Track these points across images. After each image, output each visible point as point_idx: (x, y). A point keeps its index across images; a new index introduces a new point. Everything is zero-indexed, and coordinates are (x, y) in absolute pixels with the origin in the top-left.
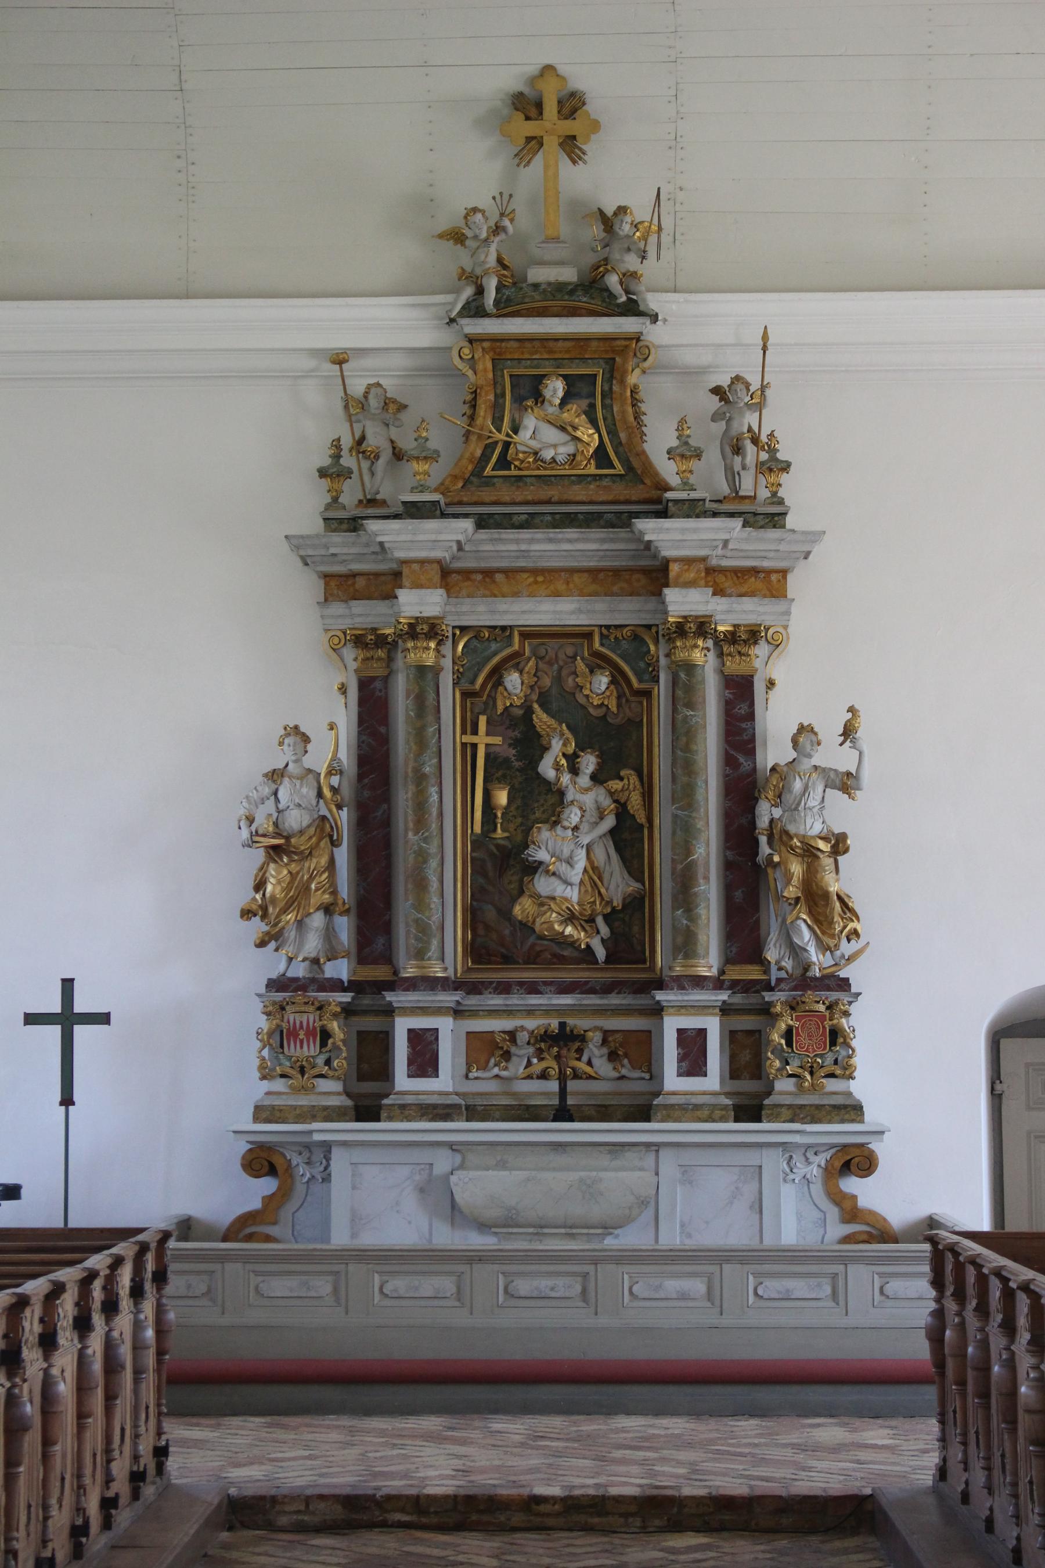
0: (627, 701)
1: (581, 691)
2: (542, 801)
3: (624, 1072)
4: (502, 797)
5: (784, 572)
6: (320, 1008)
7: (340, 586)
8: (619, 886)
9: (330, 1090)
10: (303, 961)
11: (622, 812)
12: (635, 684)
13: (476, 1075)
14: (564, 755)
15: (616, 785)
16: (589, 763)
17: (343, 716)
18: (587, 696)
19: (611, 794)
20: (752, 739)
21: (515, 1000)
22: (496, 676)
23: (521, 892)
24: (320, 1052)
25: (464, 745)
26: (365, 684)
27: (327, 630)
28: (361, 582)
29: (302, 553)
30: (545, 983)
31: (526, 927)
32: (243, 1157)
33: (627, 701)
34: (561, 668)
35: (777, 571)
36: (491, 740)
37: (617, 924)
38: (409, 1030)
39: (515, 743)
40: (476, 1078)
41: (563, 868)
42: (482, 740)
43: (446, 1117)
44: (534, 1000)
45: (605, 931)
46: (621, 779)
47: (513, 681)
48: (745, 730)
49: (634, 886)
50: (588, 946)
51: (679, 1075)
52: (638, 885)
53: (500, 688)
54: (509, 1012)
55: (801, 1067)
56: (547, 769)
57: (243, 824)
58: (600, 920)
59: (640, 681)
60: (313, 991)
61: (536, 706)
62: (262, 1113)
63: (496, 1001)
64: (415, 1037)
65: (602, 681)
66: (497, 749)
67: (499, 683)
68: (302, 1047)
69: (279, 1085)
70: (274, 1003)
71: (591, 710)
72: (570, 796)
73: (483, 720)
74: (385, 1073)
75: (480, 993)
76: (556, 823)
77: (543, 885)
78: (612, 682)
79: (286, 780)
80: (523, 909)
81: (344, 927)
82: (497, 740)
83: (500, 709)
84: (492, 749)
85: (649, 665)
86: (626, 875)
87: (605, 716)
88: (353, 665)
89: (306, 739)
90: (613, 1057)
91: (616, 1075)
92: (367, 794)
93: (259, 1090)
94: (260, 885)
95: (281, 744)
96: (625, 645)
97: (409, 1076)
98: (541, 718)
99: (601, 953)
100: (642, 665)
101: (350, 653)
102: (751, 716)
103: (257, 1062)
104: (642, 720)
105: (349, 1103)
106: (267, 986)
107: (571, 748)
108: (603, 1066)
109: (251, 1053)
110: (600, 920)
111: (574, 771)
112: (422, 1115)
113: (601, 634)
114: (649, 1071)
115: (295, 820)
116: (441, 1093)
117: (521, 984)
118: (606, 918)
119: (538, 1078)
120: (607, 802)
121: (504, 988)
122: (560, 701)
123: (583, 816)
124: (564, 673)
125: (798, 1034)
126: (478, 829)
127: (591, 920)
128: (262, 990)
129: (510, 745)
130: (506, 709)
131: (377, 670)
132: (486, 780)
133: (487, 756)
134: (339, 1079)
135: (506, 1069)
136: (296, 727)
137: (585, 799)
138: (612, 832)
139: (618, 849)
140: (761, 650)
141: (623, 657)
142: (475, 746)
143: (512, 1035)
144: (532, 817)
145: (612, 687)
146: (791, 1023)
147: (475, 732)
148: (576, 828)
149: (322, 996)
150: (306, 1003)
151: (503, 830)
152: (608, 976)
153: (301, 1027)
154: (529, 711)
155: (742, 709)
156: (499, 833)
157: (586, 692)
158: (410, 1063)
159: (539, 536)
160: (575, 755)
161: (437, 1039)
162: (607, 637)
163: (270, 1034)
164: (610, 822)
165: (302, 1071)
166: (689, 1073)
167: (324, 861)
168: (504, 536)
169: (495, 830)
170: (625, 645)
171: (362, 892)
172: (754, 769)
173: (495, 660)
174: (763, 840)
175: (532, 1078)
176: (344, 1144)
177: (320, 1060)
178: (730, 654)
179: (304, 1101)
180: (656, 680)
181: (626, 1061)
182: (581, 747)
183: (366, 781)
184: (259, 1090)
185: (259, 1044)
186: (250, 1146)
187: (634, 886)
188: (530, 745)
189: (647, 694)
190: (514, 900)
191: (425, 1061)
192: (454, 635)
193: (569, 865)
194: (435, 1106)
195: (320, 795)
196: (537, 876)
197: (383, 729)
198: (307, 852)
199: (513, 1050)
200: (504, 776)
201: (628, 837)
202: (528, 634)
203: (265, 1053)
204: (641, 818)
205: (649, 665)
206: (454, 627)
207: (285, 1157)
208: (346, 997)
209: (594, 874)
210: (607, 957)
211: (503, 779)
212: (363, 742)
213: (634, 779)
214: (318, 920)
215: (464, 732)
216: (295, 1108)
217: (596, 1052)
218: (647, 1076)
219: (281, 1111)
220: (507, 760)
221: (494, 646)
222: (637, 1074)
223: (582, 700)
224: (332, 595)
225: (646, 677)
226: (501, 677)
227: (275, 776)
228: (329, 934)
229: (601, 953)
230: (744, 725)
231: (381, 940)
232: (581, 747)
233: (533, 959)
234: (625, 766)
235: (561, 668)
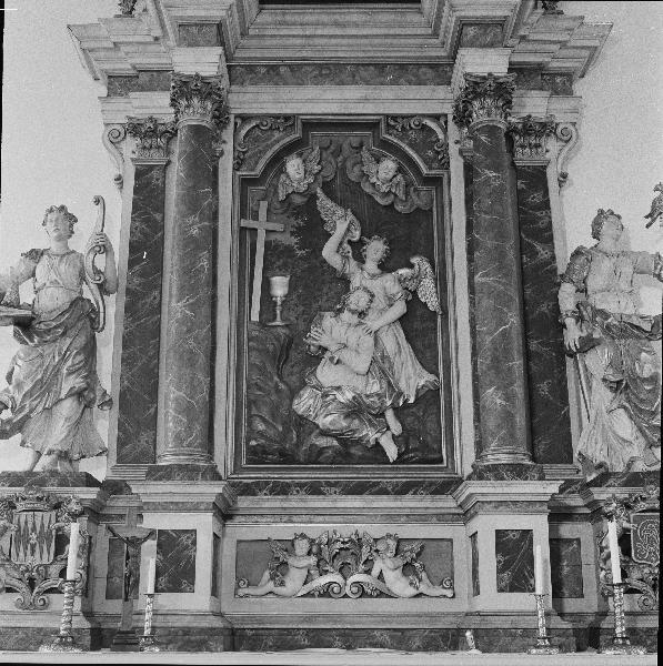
0: (415, 190)
1: (367, 180)
2: (325, 290)
3: (423, 588)
4: (280, 286)
5: (569, 76)
6: (57, 507)
7: (120, 84)
8: (412, 378)
9: (63, 611)
10: (50, 453)
11: (413, 302)
12: (425, 170)
13: (246, 591)
14: (350, 242)
15: (404, 272)
16: (376, 249)
17: (120, 207)
18: (374, 184)
19: (400, 281)
20: (549, 226)
21: (294, 502)
22: (277, 162)
23: (304, 385)
24: (55, 559)
25: (243, 230)
26: (141, 174)
27: (107, 125)
28: (144, 78)
29: (85, 45)
30: (329, 484)
31: (303, 424)
33: (415, 190)
34: (345, 160)
35: (561, 75)
36: (271, 226)
37: (409, 419)
39: (297, 232)
40: (247, 596)
41: (345, 355)
42: (261, 225)
43: (199, 646)
44: (316, 502)
45: (396, 428)
46: (411, 266)
47: (294, 166)
48: (540, 218)
49: (426, 378)
50: (377, 443)
51: (501, 590)
52: (432, 377)
53: (283, 177)
54: (289, 516)
55: (642, 580)
56: (329, 252)
58: (390, 415)
59: (430, 168)
60: (53, 485)
61: (319, 190)
63: (275, 502)
65: (388, 166)
66: (279, 237)
67: (282, 170)
71: (378, 199)
72: (356, 282)
73: (264, 205)
74: (132, 584)
75: (255, 494)
76: (340, 311)
77: (326, 374)
78: (400, 170)
79: (45, 256)
80: (305, 403)
81: (105, 427)
82: (278, 227)
83: (282, 197)
84: (273, 237)
85: (438, 153)
86: (419, 366)
87: (392, 205)
88: (128, 155)
89: (72, 219)
90: (407, 569)
91: (413, 591)
92: (136, 281)
96: (412, 135)
98: (324, 203)
99: (392, 451)
100: (430, 153)
101: (130, 145)
102: (546, 205)
104: (431, 210)
107: (356, 235)
108: (397, 582)
110: (390, 415)
111: (361, 259)
113: (388, 125)
114: (452, 587)
117: (301, 486)
118: (398, 411)
119: (320, 596)
120: (395, 289)
121: (282, 489)
122: (348, 192)
123: (371, 301)
124: (349, 164)
125: (636, 540)
126: (255, 317)
127: (382, 415)
129: (292, 234)
130: (288, 196)
131: (156, 158)
132: (265, 270)
133: (267, 245)
135: (282, 584)
136: (63, 208)
137: (375, 288)
138: (402, 320)
139: (408, 339)
140: (552, 145)
141: (410, 145)
143: (289, 546)
144: (315, 306)
145: (399, 177)
146: (625, 525)
147: (256, 218)
148: (362, 314)
150: (39, 499)
151: (283, 320)
152: (402, 477)
153: (34, 529)
154: (314, 197)
155: (537, 198)
157: (374, 180)
159: (325, 18)
160: (361, 243)
161: (194, 543)
162: (394, 127)
164: (400, 308)
165: (32, 583)
166: (513, 589)
167: (81, 341)
168: (288, 18)
169: (274, 319)
170: (412, 135)
171: (126, 382)
172: (553, 258)
173: (277, 147)
174: (570, 322)
175: (313, 596)
177: (54, 570)
178: (523, 147)
179: (32, 621)
180: (446, 166)
181: (424, 575)
182: (367, 233)
183: (137, 268)
187: (426, 378)
188: (314, 232)
189: (436, 182)
190: (294, 393)
191: (176, 574)
192: (236, 124)
193: (355, 357)
194: (187, 631)
195: (82, 278)
196: (319, 367)
197: (158, 217)
198: (61, 331)
199: (291, 561)
200: (285, 265)
201: (421, 326)
202: (312, 124)
204: (434, 304)
205: (438, 153)
206: (237, 116)
208: (91, 494)
209: (381, 366)
210: (399, 455)
211: (282, 271)
213: (426, 266)
214: (68, 407)
215: (243, 215)
217: (389, 563)
218: (449, 593)
220: (289, 250)
221: (277, 135)
222: (439, 591)
223: (368, 190)
224: (115, 93)
225: (435, 165)
226: (284, 164)
227: (35, 255)
228: (79, 425)
229: (392, 451)
230: (538, 213)
231: (144, 437)
232: (367, 233)
233: (315, 457)
234: (414, 255)
235: (345, 160)
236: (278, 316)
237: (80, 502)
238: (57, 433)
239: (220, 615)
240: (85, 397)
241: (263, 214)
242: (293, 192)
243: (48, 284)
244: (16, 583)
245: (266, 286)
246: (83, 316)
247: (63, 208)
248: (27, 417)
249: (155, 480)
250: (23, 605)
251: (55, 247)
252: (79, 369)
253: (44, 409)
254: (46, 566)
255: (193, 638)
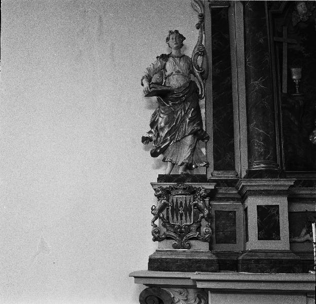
32: (141, 296)
38: (258, 207)
57: (145, 82)
60: (188, 182)
62: (155, 263)
64: (262, 211)
68: (181, 219)
69: (166, 246)
70: (162, 189)
79: (171, 59)
83: (294, 24)
89: (182, 38)
93: (151, 248)
94: (153, 124)
95: (168, 39)
97: (259, 239)
103: (151, 228)
105: (214, 258)
106: (158, 179)
109: (146, 222)
112: (271, 269)
115: (175, 82)
116: (282, 252)
126: (285, 91)
128: (155, 181)
133: (288, 50)
134: (205, 240)
142: (281, 44)
147: (281, 35)
149: (196, 185)
156: (298, 93)
158: (260, 229)
161: (278, 213)
163: (161, 210)
171: (216, 126)
176: (215, 291)
179: (182, 254)
183: (217, 64)
184: (151, 248)
185: (153, 217)
186: (146, 287)
194: (280, 262)
203: (157, 222)
207: (170, 295)
212: (215, 43)
214: (189, 140)
216: (176, 260)
219: (167, 262)
227: (164, 57)
236: (297, 90)
237: (206, 190)
238: (185, 154)
239: (297, 253)
240: (199, 136)
241: (285, 33)
242: (301, 21)
243: (174, 73)
244: (173, 234)
245: (290, 75)
246: (191, 93)
247: (177, 32)
248: (168, 145)
249: (254, 178)
250: (175, 246)
251: (174, 52)
252: (194, 119)
253: (177, 141)
254: (189, 226)
255: (285, 265)
